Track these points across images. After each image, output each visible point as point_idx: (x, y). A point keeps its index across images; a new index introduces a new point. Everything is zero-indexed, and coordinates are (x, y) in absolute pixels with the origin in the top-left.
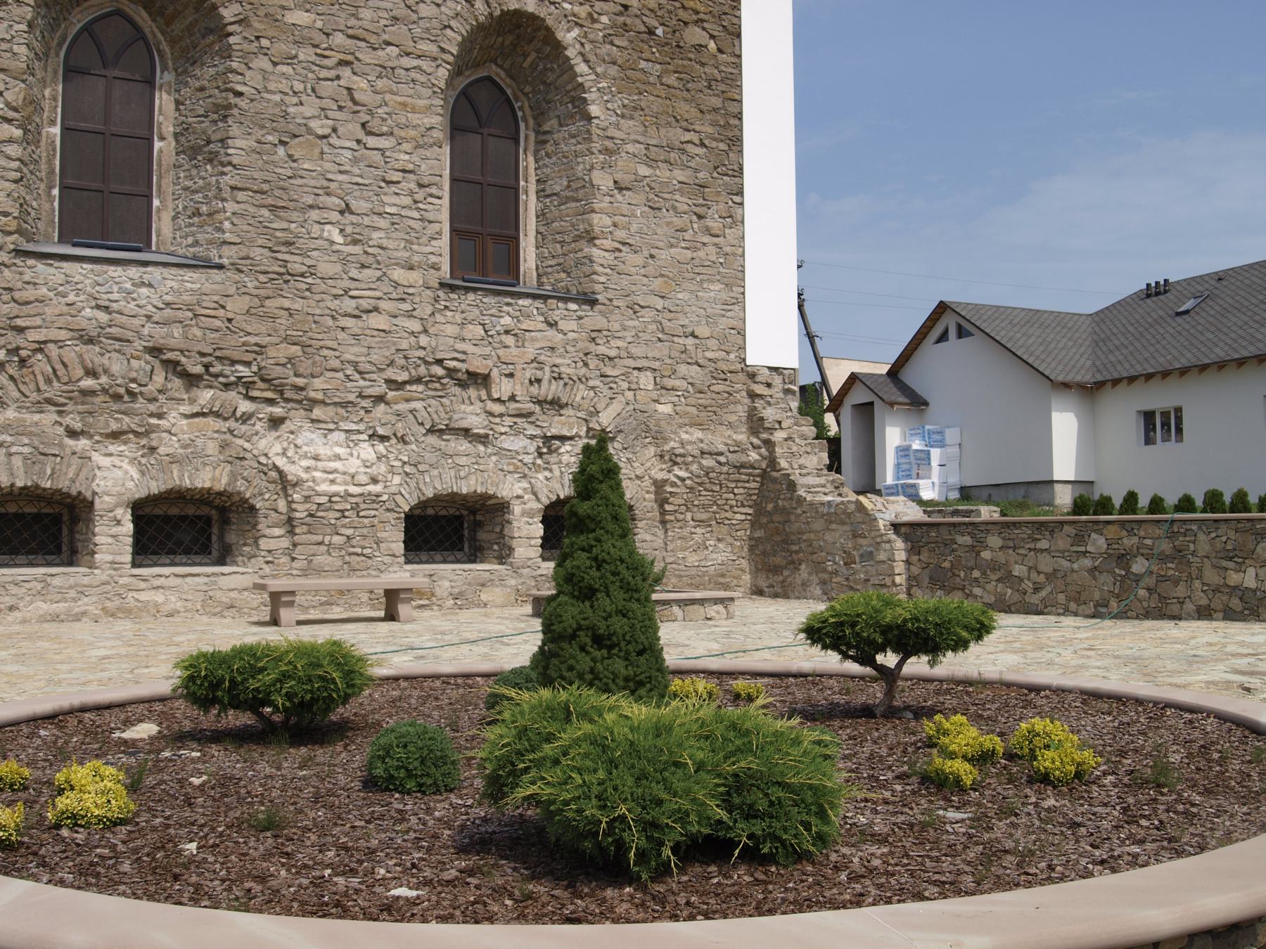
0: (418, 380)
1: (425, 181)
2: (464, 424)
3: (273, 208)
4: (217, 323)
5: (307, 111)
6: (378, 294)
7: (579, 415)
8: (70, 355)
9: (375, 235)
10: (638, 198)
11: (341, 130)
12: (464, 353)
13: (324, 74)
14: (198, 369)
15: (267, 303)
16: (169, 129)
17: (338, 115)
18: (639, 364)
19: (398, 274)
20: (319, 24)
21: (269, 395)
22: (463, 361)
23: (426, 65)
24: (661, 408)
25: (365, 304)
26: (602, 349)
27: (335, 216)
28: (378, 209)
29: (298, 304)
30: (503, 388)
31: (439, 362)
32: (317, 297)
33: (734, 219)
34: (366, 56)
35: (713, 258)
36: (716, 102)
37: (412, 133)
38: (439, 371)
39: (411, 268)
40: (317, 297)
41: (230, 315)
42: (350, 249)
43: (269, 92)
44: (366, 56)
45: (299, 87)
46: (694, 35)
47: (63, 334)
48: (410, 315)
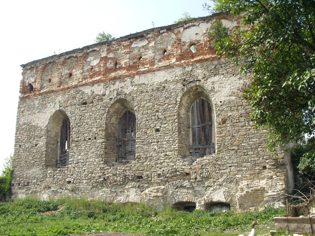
0: (175, 176)
1: (174, 131)
2: (184, 185)
7: (213, 180)
12: (184, 169)
17: (156, 122)
18: (230, 165)
21: (145, 182)
22: (184, 170)
24: (237, 176)
25: (162, 161)
26: (219, 163)
30: (193, 176)
31: (179, 171)
38: (178, 173)
39: (172, 151)
43: (143, 121)
45: (148, 119)
47: (111, 175)
48: (171, 162)
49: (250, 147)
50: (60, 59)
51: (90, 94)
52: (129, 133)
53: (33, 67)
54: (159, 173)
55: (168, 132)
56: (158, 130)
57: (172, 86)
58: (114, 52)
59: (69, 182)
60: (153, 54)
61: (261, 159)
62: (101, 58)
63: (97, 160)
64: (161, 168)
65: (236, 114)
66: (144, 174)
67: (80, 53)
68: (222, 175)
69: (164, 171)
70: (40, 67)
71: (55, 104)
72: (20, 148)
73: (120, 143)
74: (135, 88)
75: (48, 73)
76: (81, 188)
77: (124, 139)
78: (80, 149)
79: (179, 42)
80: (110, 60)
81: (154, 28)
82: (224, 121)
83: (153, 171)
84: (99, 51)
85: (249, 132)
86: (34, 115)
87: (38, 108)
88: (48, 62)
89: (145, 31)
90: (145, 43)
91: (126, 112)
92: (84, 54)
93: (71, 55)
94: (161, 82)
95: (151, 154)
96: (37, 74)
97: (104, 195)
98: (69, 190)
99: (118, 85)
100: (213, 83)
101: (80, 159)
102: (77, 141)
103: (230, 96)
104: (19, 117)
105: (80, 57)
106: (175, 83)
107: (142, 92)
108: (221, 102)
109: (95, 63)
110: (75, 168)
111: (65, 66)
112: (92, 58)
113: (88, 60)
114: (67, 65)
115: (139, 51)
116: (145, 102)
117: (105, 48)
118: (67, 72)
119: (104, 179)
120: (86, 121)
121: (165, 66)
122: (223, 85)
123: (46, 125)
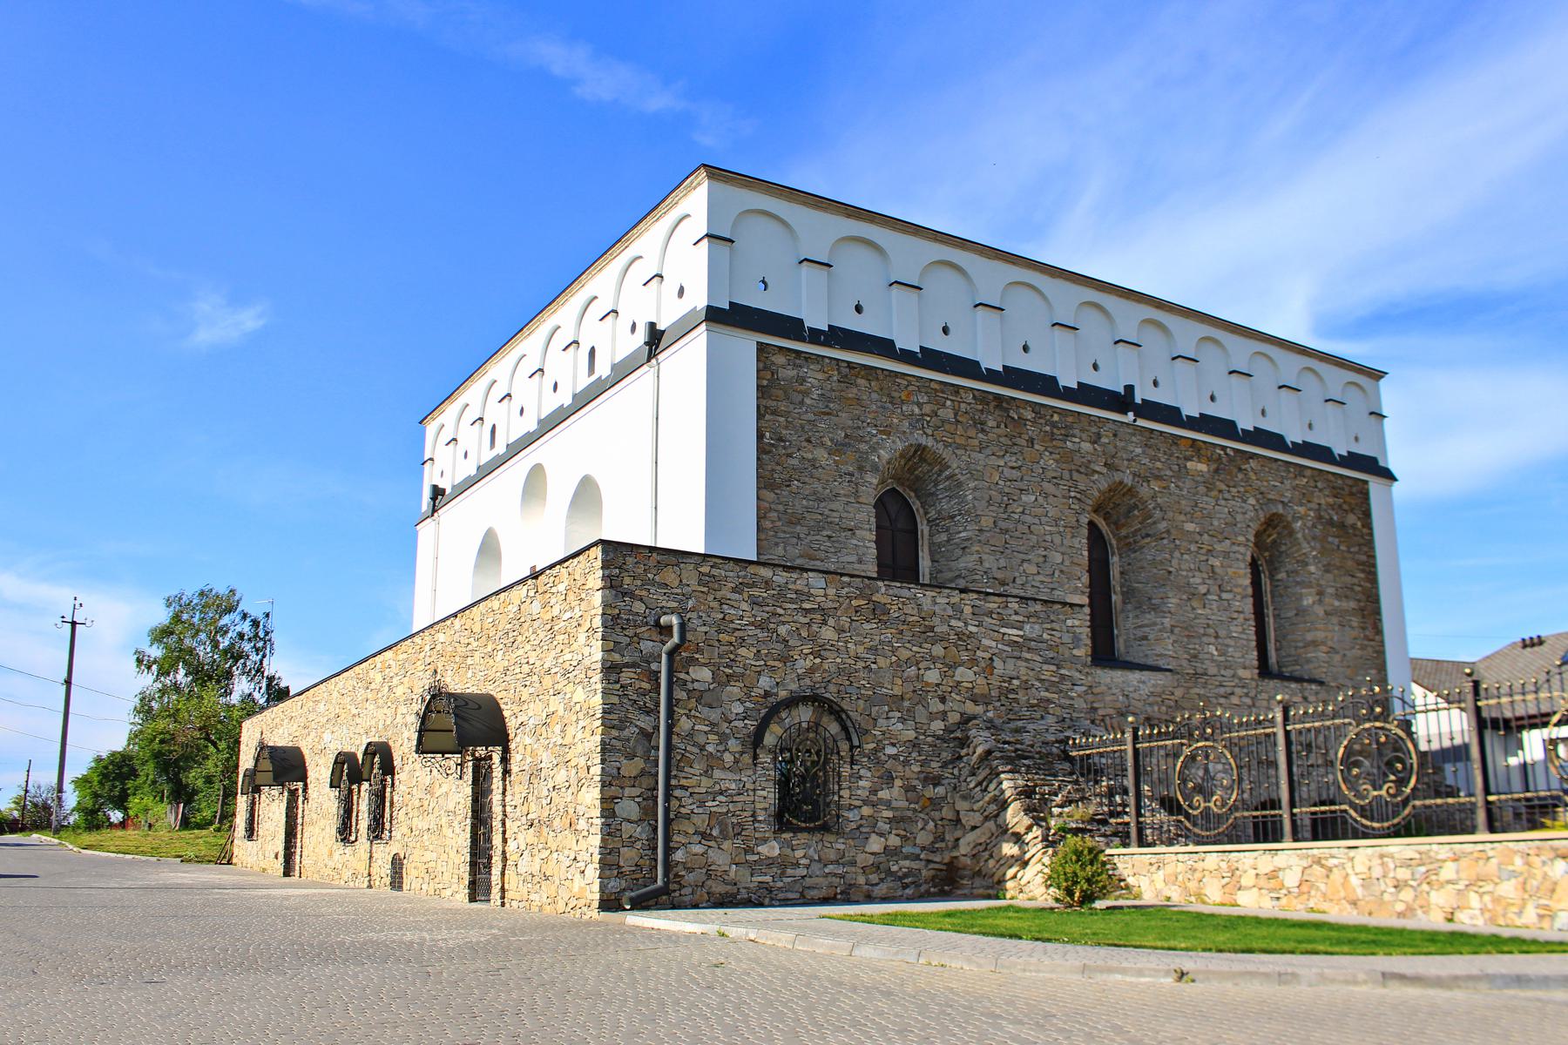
5: (1198, 580)
10: (1335, 620)
16: (1118, 589)
19: (1241, 673)
23: (1242, 549)
25: (1229, 690)
27: (1212, 640)
33: (1379, 631)
34: (1218, 547)
36: (1364, 558)
44: (1218, 547)
46: (1351, 519)
102: (1003, 583)
120: (1028, 519)
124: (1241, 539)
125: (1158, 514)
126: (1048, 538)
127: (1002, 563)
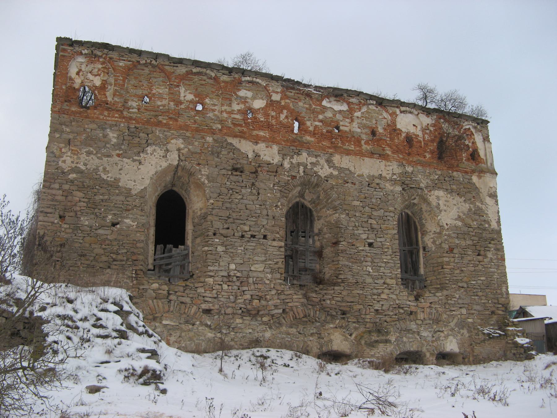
1: (394, 250)
3: (352, 262)
4: (339, 299)
5: (360, 232)
6: (384, 287)
8: (300, 311)
9: (381, 269)
11: (370, 236)
13: (364, 220)
14: (334, 313)
15: (353, 292)
18: (462, 306)
19: (388, 281)
20: (361, 205)
21: (354, 320)
24: (470, 320)
25: (380, 291)
26: (449, 302)
27: (370, 264)
28: (382, 261)
29: (361, 292)
30: (421, 316)
31: (402, 308)
32: (366, 289)
35: (481, 269)
37: (389, 236)
38: (401, 311)
40: (366, 289)
41: (343, 296)
42: (375, 274)
45: (357, 224)
48: (392, 293)
49: (479, 287)
50: (175, 68)
51: (250, 156)
52: (303, 239)
53: (96, 56)
54: (376, 308)
55: (386, 250)
56: (370, 245)
57: (389, 186)
58: (293, 100)
59: (208, 312)
60: (359, 130)
61: (490, 302)
62: (271, 101)
63: (269, 276)
64: (378, 301)
65: (463, 243)
66: (355, 308)
67: (226, 76)
68: (453, 317)
69: (382, 305)
70: (121, 64)
71: (167, 151)
72: (62, 222)
73: (289, 253)
74: (336, 173)
75: (140, 83)
76: (237, 324)
77: (297, 246)
78: (232, 250)
79: (393, 129)
80: (285, 112)
81: (362, 93)
82: (451, 250)
83: (368, 304)
84: (265, 87)
85: (476, 268)
86: (105, 159)
87: (117, 146)
88: (144, 62)
89: (347, 91)
90: (345, 107)
91: (297, 203)
92: (233, 81)
93: (204, 70)
94: (373, 176)
95: (363, 278)
96: (108, 74)
97: (287, 339)
98: (209, 327)
99: (304, 157)
100: (438, 198)
101: (235, 270)
103: (456, 219)
104: (57, 153)
105: (223, 82)
106: (393, 182)
107: (345, 181)
108: (447, 224)
109: (259, 104)
110: (221, 285)
111: (186, 84)
112: (249, 94)
113: (242, 93)
114: (189, 85)
115: (335, 115)
116: (351, 198)
117: (276, 87)
118: (190, 97)
119: (284, 310)
120: (246, 202)
121: (379, 154)
122: (447, 204)
123: (143, 188)
124: (391, 209)
125: (335, 196)
126: (259, 212)
127: (226, 226)
